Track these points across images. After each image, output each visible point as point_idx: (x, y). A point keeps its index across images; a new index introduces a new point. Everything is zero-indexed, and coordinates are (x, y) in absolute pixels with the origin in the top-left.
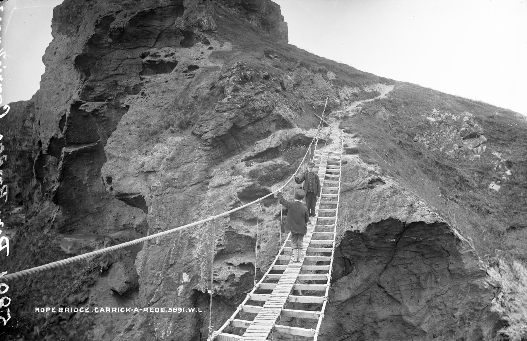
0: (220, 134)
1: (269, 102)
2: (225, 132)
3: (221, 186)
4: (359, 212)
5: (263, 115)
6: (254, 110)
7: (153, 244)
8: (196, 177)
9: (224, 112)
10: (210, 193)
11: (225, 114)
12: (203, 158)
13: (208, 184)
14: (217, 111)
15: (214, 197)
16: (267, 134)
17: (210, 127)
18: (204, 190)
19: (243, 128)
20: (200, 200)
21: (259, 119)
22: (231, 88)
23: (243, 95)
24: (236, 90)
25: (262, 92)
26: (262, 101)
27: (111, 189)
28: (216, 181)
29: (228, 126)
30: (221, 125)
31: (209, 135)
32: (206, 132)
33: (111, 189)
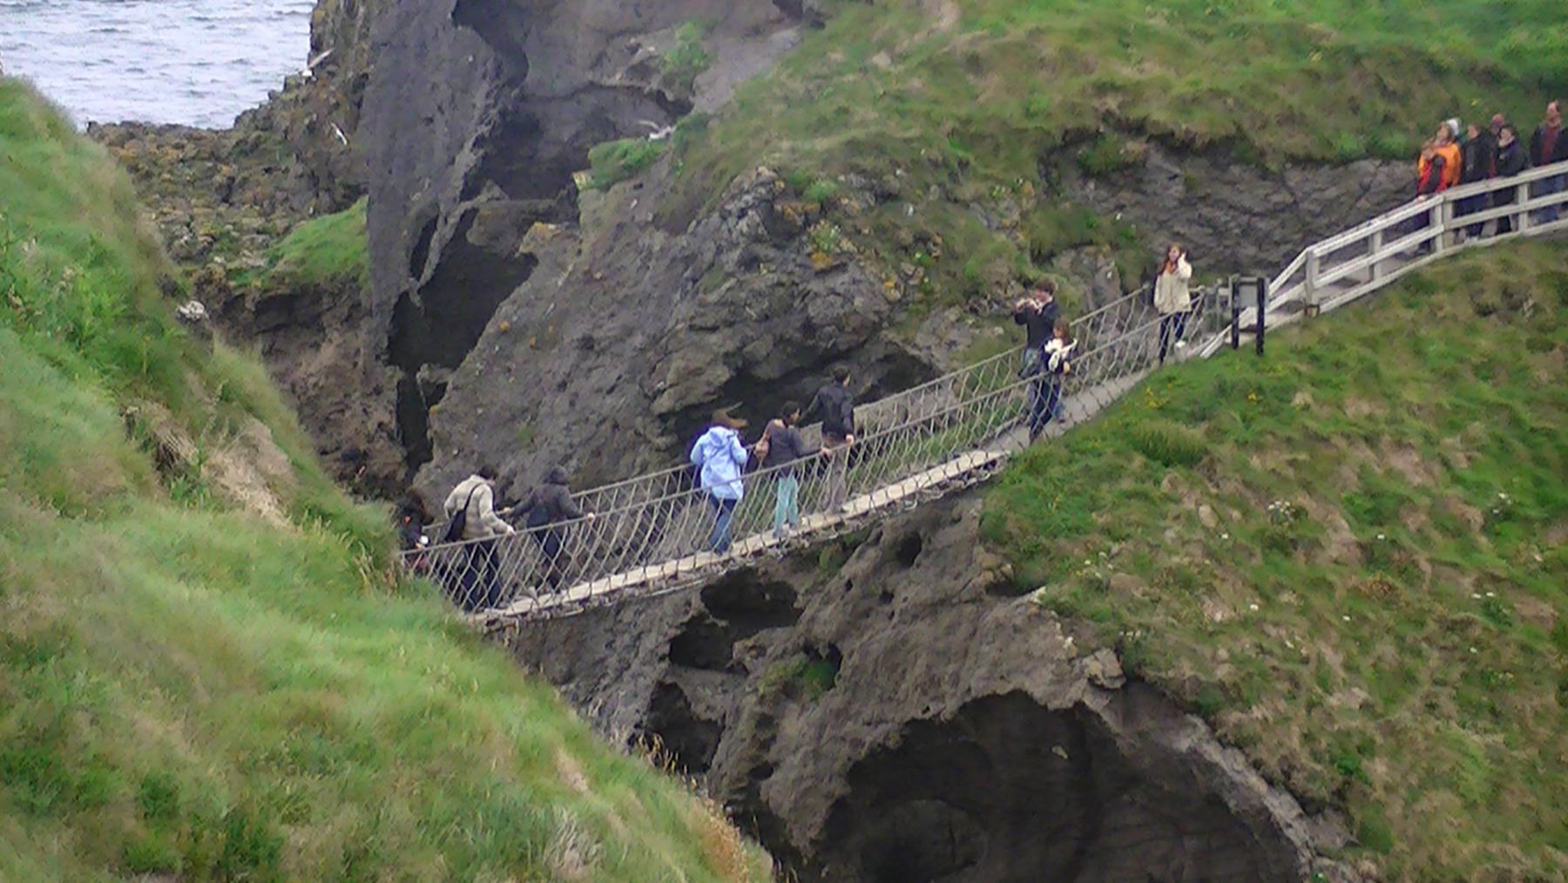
0: (692, 400)
1: (858, 302)
2: (708, 394)
4: (951, 668)
5: (844, 342)
6: (809, 327)
9: (714, 329)
11: (713, 338)
14: (691, 328)
22: (735, 255)
23: (764, 277)
24: (750, 263)
25: (841, 268)
26: (832, 298)
29: (722, 374)
30: (698, 372)
31: (664, 403)
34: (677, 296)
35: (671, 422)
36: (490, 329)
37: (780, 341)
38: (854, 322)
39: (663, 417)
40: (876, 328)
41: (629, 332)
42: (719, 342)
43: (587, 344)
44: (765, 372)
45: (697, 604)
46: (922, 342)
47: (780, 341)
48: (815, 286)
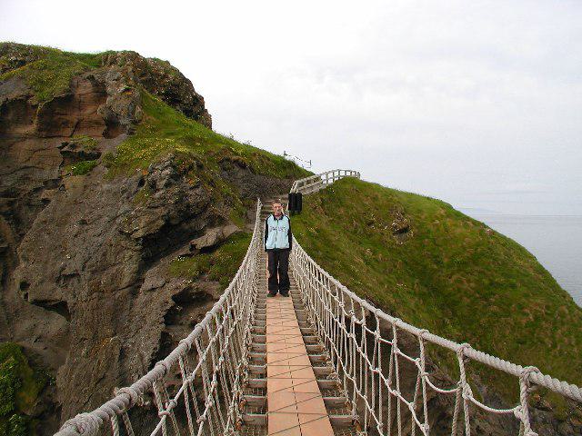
3: (153, 289)
6: (188, 206)
7: (78, 356)
8: (126, 280)
10: (142, 298)
11: (157, 210)
12: (135, 258)
13: (140, 287)
15: (146, 304)
16: (201, 233)
17: (142, 225)
18: (134, 294)
19: (176, 225)
20: (132, 305)
21: (194, 216)
23: (176, 190)
24: (168, 185)
27: (26, 296)
28: (147, 285)
29: (162, 223)
31: (140, 234)
32: (137, 230)
33: (26, 296)
34: (120, 203)
35: (140, 242)
36: (36, 221)
37: (180, 211)
38: (201, 205)
39: (137, 239)
40: (205, 208)
41: (100, 217)
42: (161, 211)
43: (83, 222)
44: (173, 222)
45: (171, 302)
46: (220, 209)
47: (180, 211)
48: (190, 192)
